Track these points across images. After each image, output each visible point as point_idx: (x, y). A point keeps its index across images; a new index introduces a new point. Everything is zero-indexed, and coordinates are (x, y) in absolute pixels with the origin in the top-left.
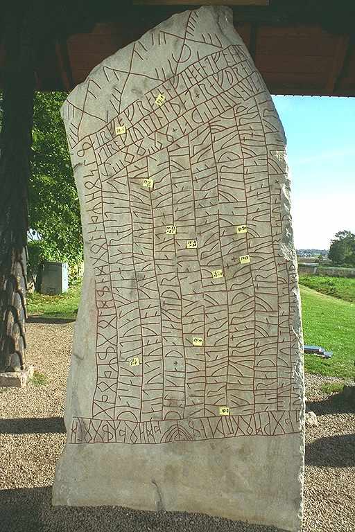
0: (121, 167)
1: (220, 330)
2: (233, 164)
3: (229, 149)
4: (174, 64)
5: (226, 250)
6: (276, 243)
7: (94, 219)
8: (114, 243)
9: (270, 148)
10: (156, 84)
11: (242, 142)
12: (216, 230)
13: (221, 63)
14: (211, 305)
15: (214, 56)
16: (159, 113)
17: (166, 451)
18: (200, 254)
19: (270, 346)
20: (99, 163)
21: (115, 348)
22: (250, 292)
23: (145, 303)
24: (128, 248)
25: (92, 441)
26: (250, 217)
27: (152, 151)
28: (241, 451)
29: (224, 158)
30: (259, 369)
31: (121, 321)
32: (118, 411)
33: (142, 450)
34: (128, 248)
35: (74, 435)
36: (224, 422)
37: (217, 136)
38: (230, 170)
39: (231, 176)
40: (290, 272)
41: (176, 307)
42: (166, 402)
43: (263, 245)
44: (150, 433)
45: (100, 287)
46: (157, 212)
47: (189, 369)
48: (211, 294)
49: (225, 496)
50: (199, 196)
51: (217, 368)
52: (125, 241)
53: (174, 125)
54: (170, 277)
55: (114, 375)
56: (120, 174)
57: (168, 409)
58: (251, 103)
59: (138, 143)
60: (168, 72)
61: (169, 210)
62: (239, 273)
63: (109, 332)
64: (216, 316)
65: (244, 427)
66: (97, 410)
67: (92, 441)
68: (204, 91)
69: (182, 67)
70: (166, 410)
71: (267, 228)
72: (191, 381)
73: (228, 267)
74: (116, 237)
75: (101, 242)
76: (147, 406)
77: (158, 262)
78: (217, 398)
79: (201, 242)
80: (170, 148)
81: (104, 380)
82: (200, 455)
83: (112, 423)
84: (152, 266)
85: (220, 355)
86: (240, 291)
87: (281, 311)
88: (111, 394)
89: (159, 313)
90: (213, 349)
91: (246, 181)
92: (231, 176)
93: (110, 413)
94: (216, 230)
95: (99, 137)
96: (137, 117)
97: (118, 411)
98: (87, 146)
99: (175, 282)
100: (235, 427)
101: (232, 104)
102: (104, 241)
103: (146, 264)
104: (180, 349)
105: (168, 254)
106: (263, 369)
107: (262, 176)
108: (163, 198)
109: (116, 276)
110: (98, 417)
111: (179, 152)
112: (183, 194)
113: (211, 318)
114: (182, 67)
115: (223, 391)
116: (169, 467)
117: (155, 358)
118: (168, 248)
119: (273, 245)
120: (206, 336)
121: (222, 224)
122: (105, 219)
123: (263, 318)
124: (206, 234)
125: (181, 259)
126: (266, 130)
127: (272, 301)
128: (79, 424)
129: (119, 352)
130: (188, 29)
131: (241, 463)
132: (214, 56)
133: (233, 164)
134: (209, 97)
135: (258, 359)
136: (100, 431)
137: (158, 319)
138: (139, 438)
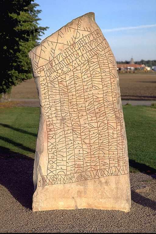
2: (97, 75)
3: (95, 70)
4: (74, 39)
5: (96, 107)
6: (114, 103)
7: (45, 97)
8: (53, 106)
9: (111, 69)
10: (67, 47)
11: (100, 67)
13: (92, 38)
14: (91, 127)
15: (89, 35)
16: (69, 57)
17: (77, 185)
18: (86, 110)
19: (114, 142)
20: (47, 76)
21: (55, 146)
23: (66, 129)
24: (59, 108)
25: (48, 184)
26: (104, 94)
27: (67, 72)
28: (106, 182)
29: (94, 73)
30: (110, 151)
31: (57, 136)
32: (57, 171)
33: (68, 186)
34: (59, 108)
35: (40, 183)
36: (99, 172)
37: (91, 65)
38: (96, 77)
39: (96, 80)
40: (120, 114)
42: (76, 166)
43: (109, 105)
44: (71, 179)
45: (48, 123)
46: (70, 94)
47: (85, 152)
48: (91, 124)
49: (101, 200)
50: (85, 87)
51: (95, 151)
52: (58, 105)
53: (75, 62)
54: (75, 118)
55: (55, 157)
56: (55, 80)
57: (77, 169)
58: (103, 52)
59: (62, 69)
60: (72, 42)
61: (74, 93)
62: (101, 115)
63: (53, 141)
64: (94, 132)
65: (106, 173)
66: (49, 172)
67: (48, 184)
68: (86, 49)
69: (77, 40)
71: (111, 98)
72: (85, 157)
73: (97, 113)
74: (54, 104)
75: (48, 106)
76: (69, 168)
77: (71, 113)
78: (96, 163)
79: (87, 104)
80: (74, 71)
81: (52, 160)
82: (90, 185)
83: (55, 176)
84: (68, 114)
85: (96, 146)
86: (102, 122)
87: (118, 129)
91: (103, 81)
92: (96, 80)
93: (54, 172)
95: (47, 67)
96: (61, 59)
98: (41, 70)
99: (77, 120)
100: (103, 173)
101: (96, 53)
102: (49, 105)
103: (66, 113)
104: (81, 145)
105: (74, 109)
107: (108, 79)
108: (71, 89)
109: (54, 119)
110: (50, 174)
112: (79, 87)
113: (92, 132)
114: (77, 40)
115: (98, 160)
116: (79, 191)
117: (71, 149)
118: (74, 107)
120: (90, 139)
122: (49, 97)
123: (111, 131)
125: (80, 111)
126: (109, 62)
127: (114, 125)
128: (42, 178)
129: (57, 148)
130: (79, 26)
131: (106, 187)
132: (89, 35)
133: (97, 75)
134: (87, 51)
135: (110, 147)
136: (51, 180)
137: (71, 134)
138: (66, 181)
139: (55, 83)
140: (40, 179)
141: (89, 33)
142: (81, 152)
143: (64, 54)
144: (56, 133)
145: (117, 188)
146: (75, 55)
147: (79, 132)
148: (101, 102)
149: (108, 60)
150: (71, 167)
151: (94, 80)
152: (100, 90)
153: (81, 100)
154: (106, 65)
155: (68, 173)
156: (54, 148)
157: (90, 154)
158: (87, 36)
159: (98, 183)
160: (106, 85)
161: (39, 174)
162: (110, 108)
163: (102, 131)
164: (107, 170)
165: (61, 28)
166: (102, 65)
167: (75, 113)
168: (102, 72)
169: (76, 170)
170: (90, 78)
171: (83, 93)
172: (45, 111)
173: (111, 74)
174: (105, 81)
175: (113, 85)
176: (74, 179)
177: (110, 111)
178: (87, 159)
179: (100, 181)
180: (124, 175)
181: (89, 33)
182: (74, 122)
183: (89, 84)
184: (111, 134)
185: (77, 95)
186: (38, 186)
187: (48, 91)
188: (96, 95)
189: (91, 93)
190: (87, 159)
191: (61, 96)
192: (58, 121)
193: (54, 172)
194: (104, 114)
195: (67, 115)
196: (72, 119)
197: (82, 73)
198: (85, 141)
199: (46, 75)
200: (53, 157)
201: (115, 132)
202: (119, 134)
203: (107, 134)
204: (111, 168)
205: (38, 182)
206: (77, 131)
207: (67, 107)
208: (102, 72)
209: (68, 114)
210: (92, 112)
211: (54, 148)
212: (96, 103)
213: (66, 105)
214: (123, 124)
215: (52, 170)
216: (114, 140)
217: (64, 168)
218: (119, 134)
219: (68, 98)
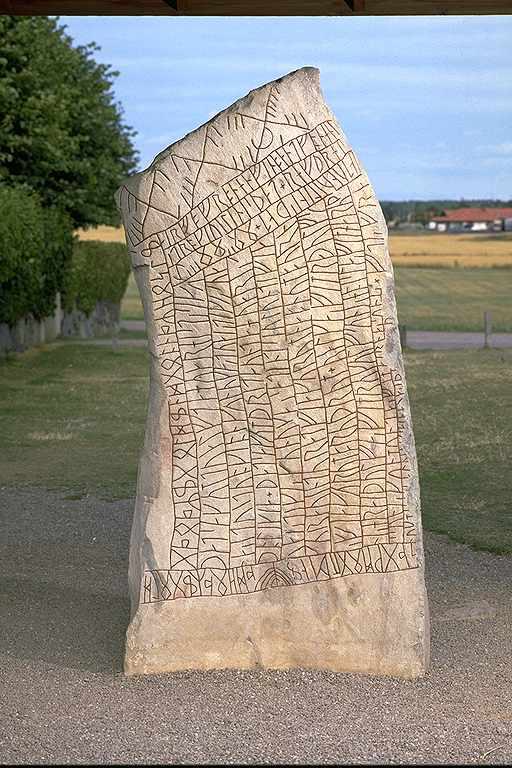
0: (197, 270)
1: (320, 452)
2: (325, 262)
4: (254, 152)
7: (166, 329)
9: (367, 243)
10: (231, 173)
11: (336, 237)
12: (310, 338)
16: (239, 208)
17: (262, 601)
18: (292, 368)
21: (196, 481)
22: (352, 407)
23: (229, 426)
27: (233, 252)
28: (351, 592)
29: (316, 256)
31: (202, 449)
32: (202, 557)
33: (232, 603)
36: (329, 560)
37: (308, 231)
39: (323, 276)
40: (396, 383)
41: (266, 429)
42: (260, 542)
43: (363, 354)
45: (175, 409)
46: (241, 320)
47: (285, 499)
48: (307, 412)
50: (290, 299)
52: (203, 354)
54: (258, 393)
55: (196, 513)
57: (263, 550)
58: (344, 192)
59: (216, 243)
60: (248, 161)
61: (254, 317)
63: (188, 463)
64: (314, 436)
65: (351, 563)
69: (263, 154)
70: (260, 551)
74: (190, 349)
77: (245, 377)
79: (293, 355)
81: (183, 521)
82: (303, 599)
83: (194, 573)
85: (322, 481)
86: (340, 407)
88: (194, 540)
89: (246, 437)
90: (313, 475)
92: (323, 276)
93: (193, 560)
94: (310, 338)
97: (202, 557)
100: (342, 564)
101: (323, 195)
106: (370, 496)
107: (359, 275)
109: (192, 395)
110: (177, 567)
111: (266, 251)
114: (263, 154)
119: (375, 352)
121: (317, 330)
123: (367, 435)
124: (297, 344)
126: (363, 223)
127: (377, 416)
131: (349, 607)
132: (299, 139)
133: (325, 262)
139: (195, 284)
140: (148, 580)
141: (301, 132)
142: (275, 499)
143: (223, 198)
144: (198, 436)
145: (385, 611)
146: (258, 200)
147: (270, 436)
148: (337, 344)
149: (360, 215)
150: (245, 543)
151: (315, 276)
152: (332, 308)
153: (275, 339)
154: (355, 233)
155: (235, 563)
156: (189, 484)
157: (301, 505)
158: (295, 142)
159: (328, 596)
160: (352, 294)
161: (146, 566)
162: (365, 365)
163: (341, 434)
164: (355, 554)
165: (219, 115)
166: (341, 231)
167: (258, 378)
168: (340, 253)
169: (258, 557)
170: (305, 270)
171: (280, 316)
172: (165, 372)
173: (368, 258)
174: (350, 280)
175: (373, 292)
176: (253, 584)
177: (366, 373)
178: (292, 521)
179: (334, 592)
180: (407, 571)
181: (301, 132)
182: (254, 407)
183: (298, 289)
184: (369, 446)
185: (263, 323)
186: (142, 601)
187: (175, 310)
188: (320, 323)
189: (304, 316)
190: (292, 521)
192: (204, 404)
193: (193, 560)
194: (347, 382)
195: (230, 385)
196: (247, 396)
197: (278, 254)
198: (288, 464)
199: (169, 261)
200: (188, 514)
201: (381, 439)
202: (392, 443)
203: (354, 445)
204: (365, 550)
206: (263, 434)
207: (232, 359)
208: (340, 253)
210: (308, 376)
212: (320, 350)
213: (231, 353)
214: (405, 414)
215: (184, 553)
216: (377, 462)
217: (222, 546)
218: (392, 443)
219: (234, 331)
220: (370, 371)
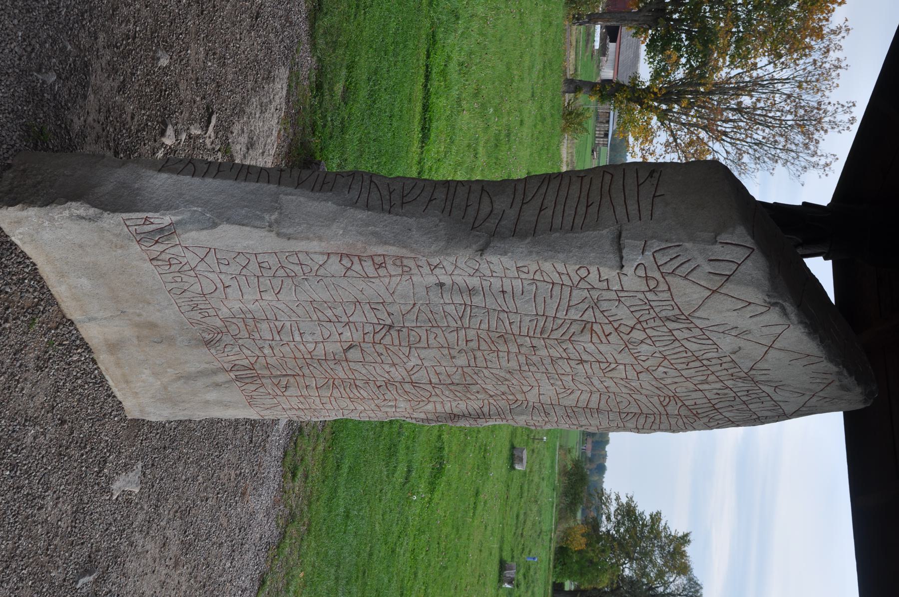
34: (477, 300)
103: (457, 318)
140: (157, 221)
186: (125, 216)
191: (529, 318)
192: (422, 292)
199: (626, 294)
205: (144, 215)
209: (453, 324)
211: (307, 269)
220: (479, 411)
